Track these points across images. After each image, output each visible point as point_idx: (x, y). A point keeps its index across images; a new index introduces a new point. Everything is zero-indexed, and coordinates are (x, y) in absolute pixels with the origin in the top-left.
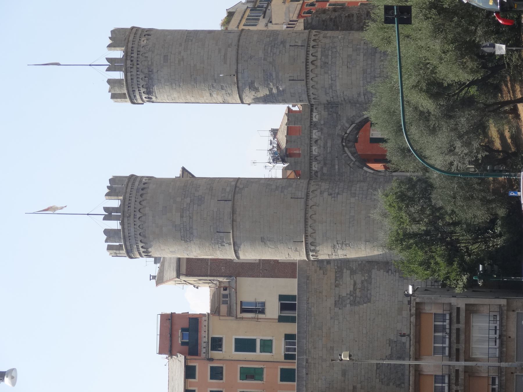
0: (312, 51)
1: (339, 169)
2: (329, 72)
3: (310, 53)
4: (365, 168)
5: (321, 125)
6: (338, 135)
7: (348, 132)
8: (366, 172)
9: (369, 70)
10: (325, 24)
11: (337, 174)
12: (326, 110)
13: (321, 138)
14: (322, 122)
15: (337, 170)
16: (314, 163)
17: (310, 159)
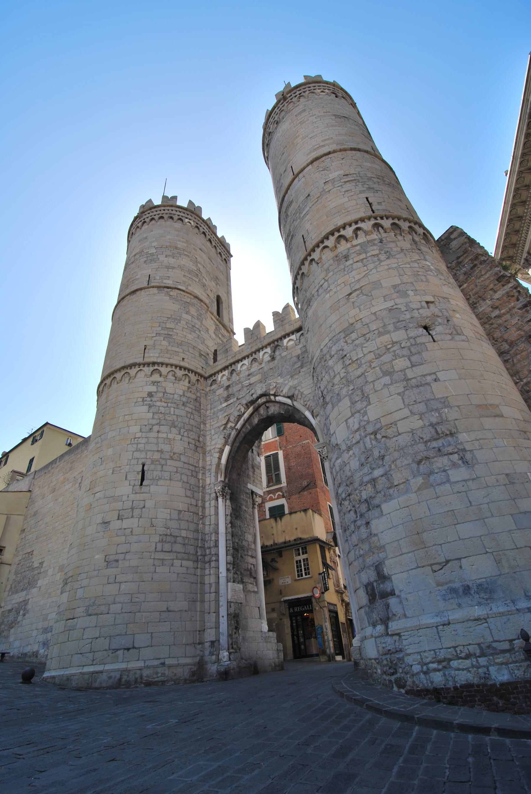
0: (367, 226)
1: (221, 410)
2: (332, 273)
3: (360, 225)
4: (227, 449)
5: (280, 355)
6: (270, 384)
7: (278, 398)
8: (221, 451)
9: (354, 336)
10: (460, 260)
11: (216, 410)
12: (304, 349)
13: (261, 364)
14: (284, 354)
15: (220, 407)
16: (226, 373)
17: (231, 365)
